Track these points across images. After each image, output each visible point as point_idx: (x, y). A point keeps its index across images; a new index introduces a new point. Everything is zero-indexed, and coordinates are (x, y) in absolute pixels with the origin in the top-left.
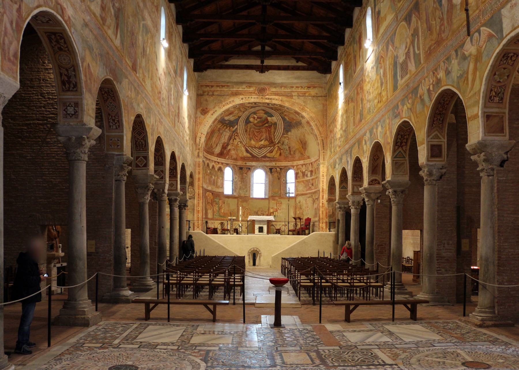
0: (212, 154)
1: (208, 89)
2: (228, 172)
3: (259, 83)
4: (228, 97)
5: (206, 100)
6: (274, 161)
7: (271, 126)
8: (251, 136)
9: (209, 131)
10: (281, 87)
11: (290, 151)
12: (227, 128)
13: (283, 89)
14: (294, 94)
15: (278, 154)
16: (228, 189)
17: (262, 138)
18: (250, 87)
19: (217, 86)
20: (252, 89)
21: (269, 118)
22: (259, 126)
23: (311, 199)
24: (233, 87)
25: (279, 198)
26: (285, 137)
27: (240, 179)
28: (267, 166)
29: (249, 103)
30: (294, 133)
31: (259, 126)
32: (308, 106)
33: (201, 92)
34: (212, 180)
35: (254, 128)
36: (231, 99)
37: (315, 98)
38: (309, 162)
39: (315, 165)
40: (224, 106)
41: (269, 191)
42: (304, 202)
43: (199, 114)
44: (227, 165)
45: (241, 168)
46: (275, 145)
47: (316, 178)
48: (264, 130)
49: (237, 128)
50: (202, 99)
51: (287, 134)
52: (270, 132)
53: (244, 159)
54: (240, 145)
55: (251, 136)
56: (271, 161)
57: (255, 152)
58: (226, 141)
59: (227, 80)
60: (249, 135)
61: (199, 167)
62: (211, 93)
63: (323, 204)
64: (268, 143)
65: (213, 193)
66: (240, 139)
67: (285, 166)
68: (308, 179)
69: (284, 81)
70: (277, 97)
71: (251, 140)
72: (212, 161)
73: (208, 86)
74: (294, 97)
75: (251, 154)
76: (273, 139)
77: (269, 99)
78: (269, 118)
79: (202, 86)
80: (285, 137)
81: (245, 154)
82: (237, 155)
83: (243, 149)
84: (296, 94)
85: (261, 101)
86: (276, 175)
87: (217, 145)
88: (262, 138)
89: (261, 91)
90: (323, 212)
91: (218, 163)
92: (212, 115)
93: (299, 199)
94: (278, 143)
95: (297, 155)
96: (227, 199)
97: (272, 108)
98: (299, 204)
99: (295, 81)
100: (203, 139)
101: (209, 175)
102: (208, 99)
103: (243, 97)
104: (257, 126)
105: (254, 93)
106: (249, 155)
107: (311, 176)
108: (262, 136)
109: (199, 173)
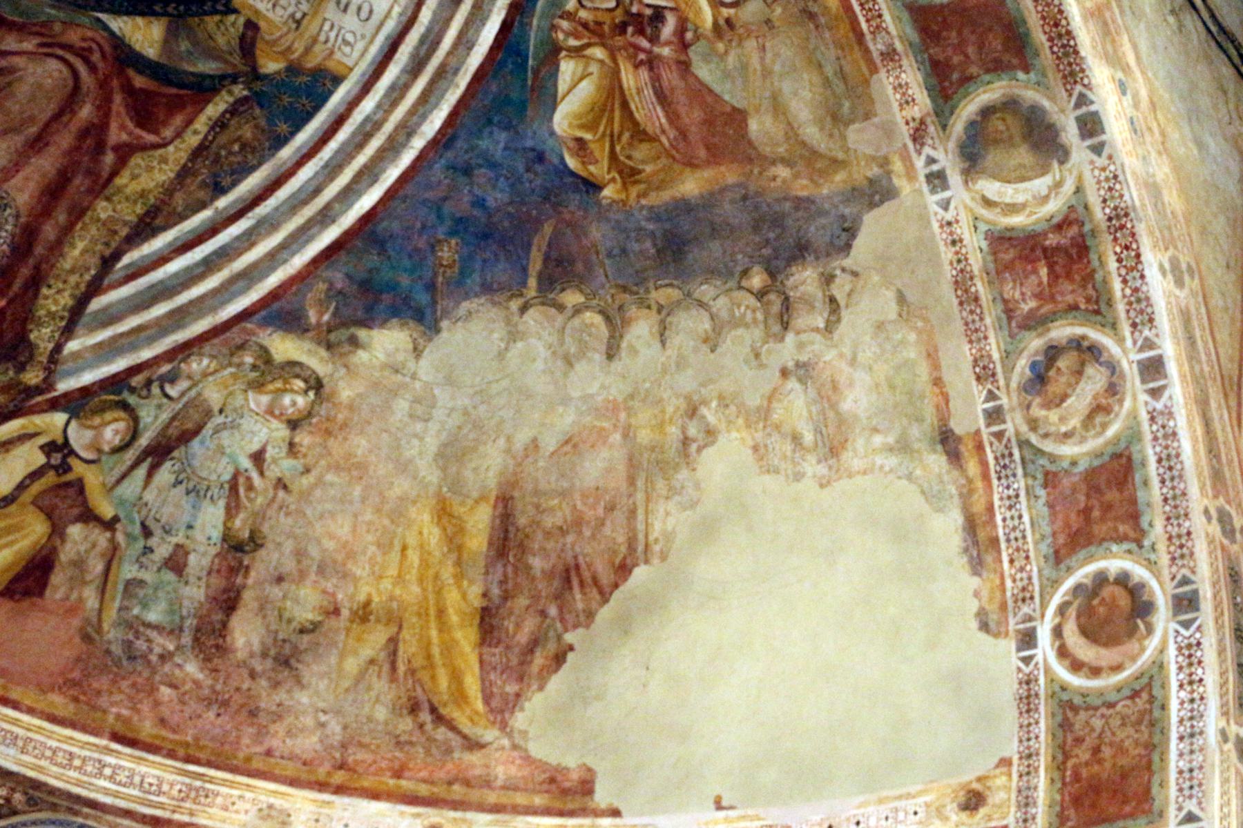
7: (204, 89)
11: (229, 602)
26: (268, 371)
51: (338, 336)
76: (55, 300)
80: (268, 371)
94: (79, 404)
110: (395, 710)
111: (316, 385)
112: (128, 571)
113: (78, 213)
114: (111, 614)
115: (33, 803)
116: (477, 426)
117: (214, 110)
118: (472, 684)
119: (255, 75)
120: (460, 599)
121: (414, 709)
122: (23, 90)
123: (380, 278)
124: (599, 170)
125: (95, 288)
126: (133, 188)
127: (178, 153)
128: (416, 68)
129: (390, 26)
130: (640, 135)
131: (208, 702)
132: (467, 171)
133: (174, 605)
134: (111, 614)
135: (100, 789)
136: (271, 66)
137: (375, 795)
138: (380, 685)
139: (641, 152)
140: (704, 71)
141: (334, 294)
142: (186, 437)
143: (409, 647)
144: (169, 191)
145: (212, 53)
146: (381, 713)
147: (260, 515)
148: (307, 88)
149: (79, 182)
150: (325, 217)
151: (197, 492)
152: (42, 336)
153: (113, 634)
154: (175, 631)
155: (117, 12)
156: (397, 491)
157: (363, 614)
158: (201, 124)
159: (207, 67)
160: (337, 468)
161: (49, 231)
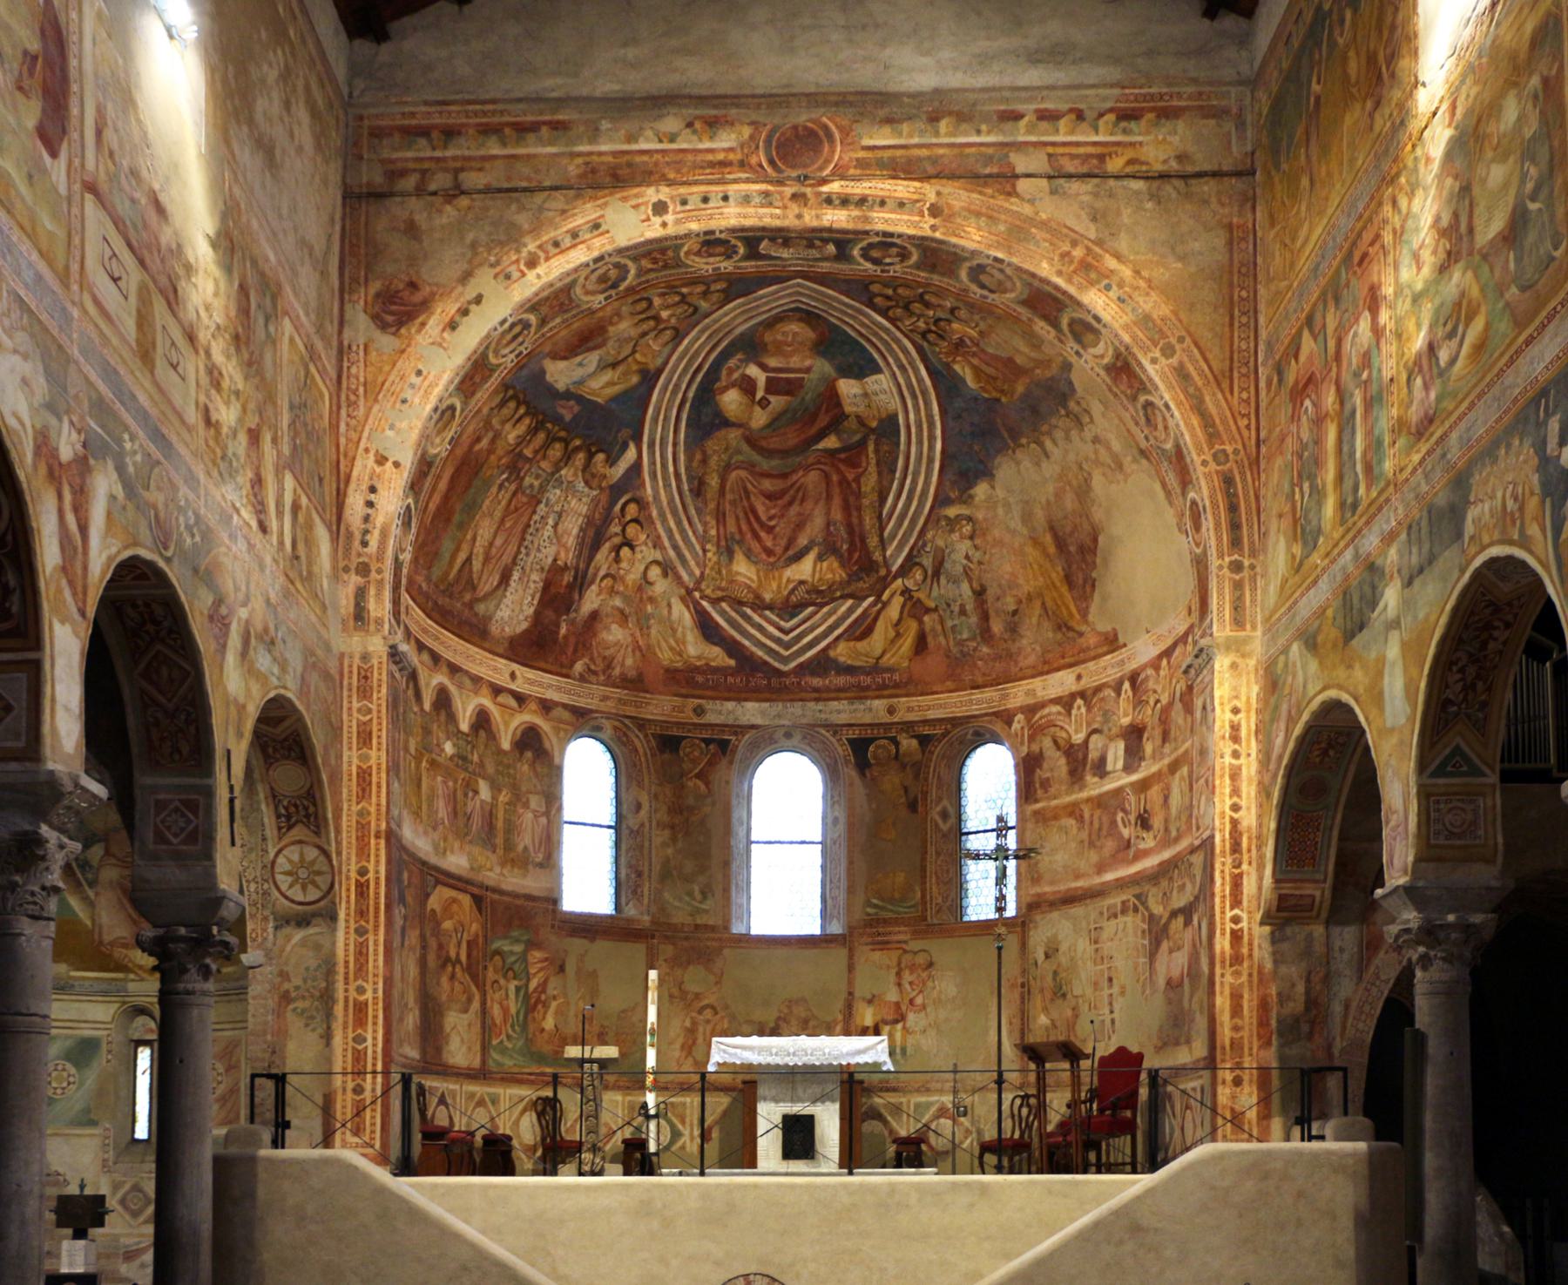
0: (475, 631)
1: (422, 149)
2: (588, 775)
3: (777, 100)
4: (558, 201)
5: (411, 230)
6: (881, 690)
7: (862, 444)
8: (731, 527)
9: (439, 448)
10: (934, 119)
12: (567, 457)
13: (947, 135)
14: (1021, 163)
15: (908, 643)
16: (587, 880)
17: (803, 541)
18: (713, 124)
19: (486, 131)
20: (725, 141)
21: (848, 388)
22: (784, 453)
23: (1131, 924)
24: (594, 134)
25: (917, 934)
26: (953, 523)
27: (663, 815)
28: (835, 729)
29: (711, 243)
30: (1018, 486)
31: (784, 453)
32: (1123, 244)
33: (371, 175)
34: (474, 805)
35: (750, 466)
36: (583, 215)
37: (1168, 189)
38: (1113, 674)
39: (1162, 687)
40: (532, 263)
41: (851, 890)
42: (1083, 946)
43: (361, 325)
44: (582, 721)
45: (669, 743)
46: (884, 583)
47: (1174, 767)
48: (812, 478)
49: (636, 467)
50: (381, 224)
51: (966, 499)
52: (851, 505)
53: (686, 679)
54: (661, 586)
55: (731, 527)
56: (860, 693)
57: (762, 635)
58: (568, 557)
59: (554, 85)
60: (720, 517)
61: (365, 692)
62: (440, 181)
63: (1236, 936)
64: (841, 575)
65: (482, 897)
66: (657, 544)
67: (955, 722)
68: (1109, 786)
69: (955, 80)
70: (902, 189)
71: (730, 554)
72: (477, 680)
73: (425, 132)
74: (1023, 185)
75: (732, 648)
76: (873, 542)
77: (845, 201)
78: (848, 388)
79: (377, 134)
80: (953, 523)
81: (695, 648)
82: (644, 653)
83: (682, 615)
84: (1033, 162)
85: (790, 221)
86: (892, 781)
87: (505, 578)
88: (803, 541)
89: (794, 150)
90: (1236, 997)
91: (520, 698)
92: (452, 326)
93: (1056, 927)
94: (904, 571)
95: (1033, 639)
96: (577, 944)
97: (861, 289)
98: (1046, 968)
99: (1033, 76)
100: (392, 500)
101: (448, 774)
102: (421, 218)
103: (664, 194)
104: (768, 453)
105: (742, 164)
106: (717, 656)
107: (1128, 769)
108: (800, 526)
109: (365, 737)
110: (1054, 631)
111: (970, 519)
112: (949, 623)
113: (859, 509)
114: (951, 643)
115: (954, 726)
116: (1027, 502)
117: (871, 448)
118: (1074, 611)
119: (873, 430)
120: (1057, 574)
121: (1060, 628)
122: (811, 487)
123: (965, 467)
124: (995, 394)
125: (882, 529)
126: (868, 489)
127: (872, 469)
128: (914, 397)
129: (894, 390)
130: (995, 379)
131: (994, 660)
132: (959, 416)
133: (969, 628)
134: (951, 643)
135: (975, 710)
136: (874, 424)
137: (1058, 669)
138: (1046, 624)
139: (999, 383)
140: (991, 351)
141: (954, 483)
142: (941, 563)
143: (1049, 604)
144: (880, 481)
145: (855, 432)
146: (1050, 635)
147: (980, 578)
148: (892, 419)
149: (852, 499)
150: (931, 460)
151: (956, 581)
152: (877, 556)
153: (955, 650)
154: (973, 639)
155: (817, 442)
156: (1016, 545)
157: (1030, 598)
158: (871, 455)
159: (857, 437)
160: (993, 547)
161: (855, 521)
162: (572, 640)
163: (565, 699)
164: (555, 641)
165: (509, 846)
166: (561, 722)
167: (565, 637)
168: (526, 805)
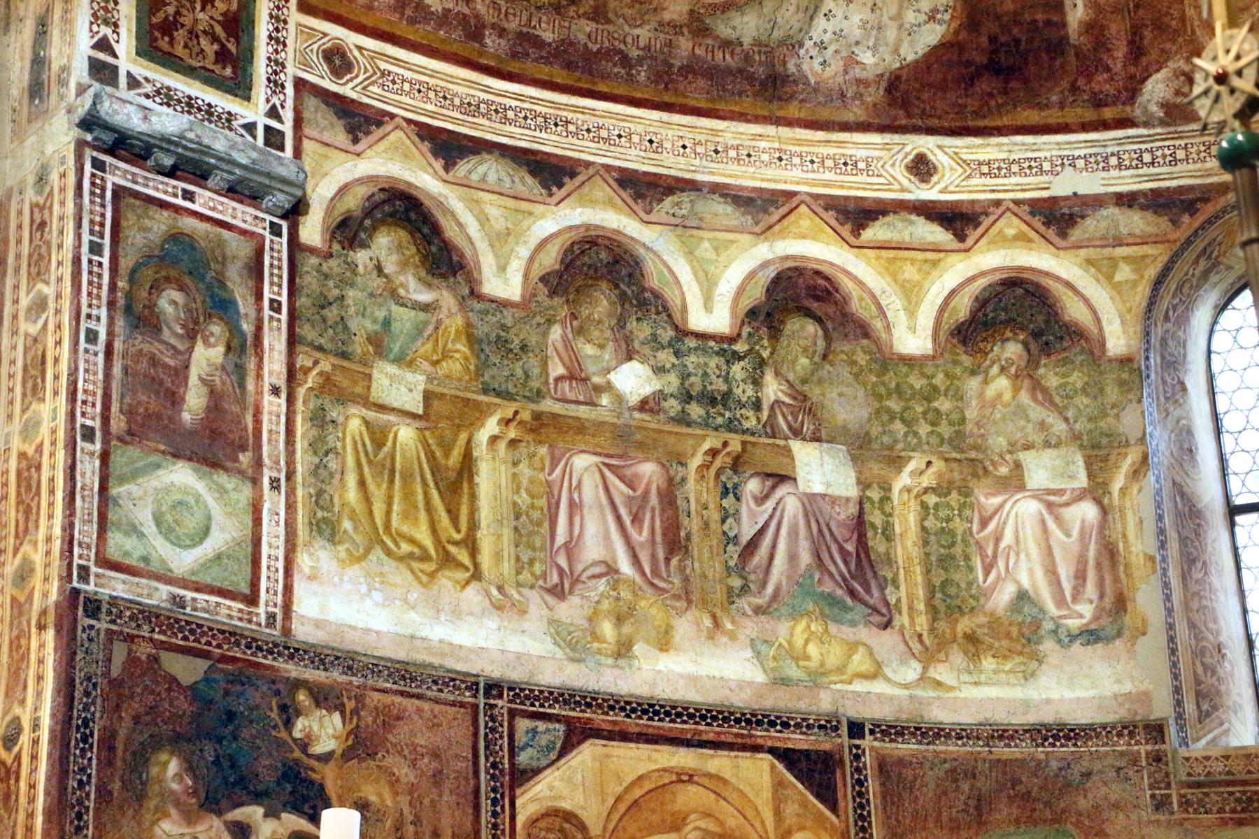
91: (959, 220)
162: (1117, 30)
163: (1127, 182)
164: (1058, 46)
165: (948, 600)
166: (1119, 242)
167: (1090, 27)
168: (1015, 482)
